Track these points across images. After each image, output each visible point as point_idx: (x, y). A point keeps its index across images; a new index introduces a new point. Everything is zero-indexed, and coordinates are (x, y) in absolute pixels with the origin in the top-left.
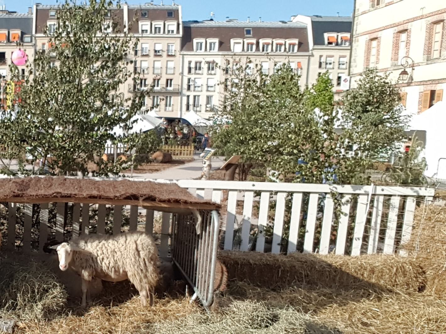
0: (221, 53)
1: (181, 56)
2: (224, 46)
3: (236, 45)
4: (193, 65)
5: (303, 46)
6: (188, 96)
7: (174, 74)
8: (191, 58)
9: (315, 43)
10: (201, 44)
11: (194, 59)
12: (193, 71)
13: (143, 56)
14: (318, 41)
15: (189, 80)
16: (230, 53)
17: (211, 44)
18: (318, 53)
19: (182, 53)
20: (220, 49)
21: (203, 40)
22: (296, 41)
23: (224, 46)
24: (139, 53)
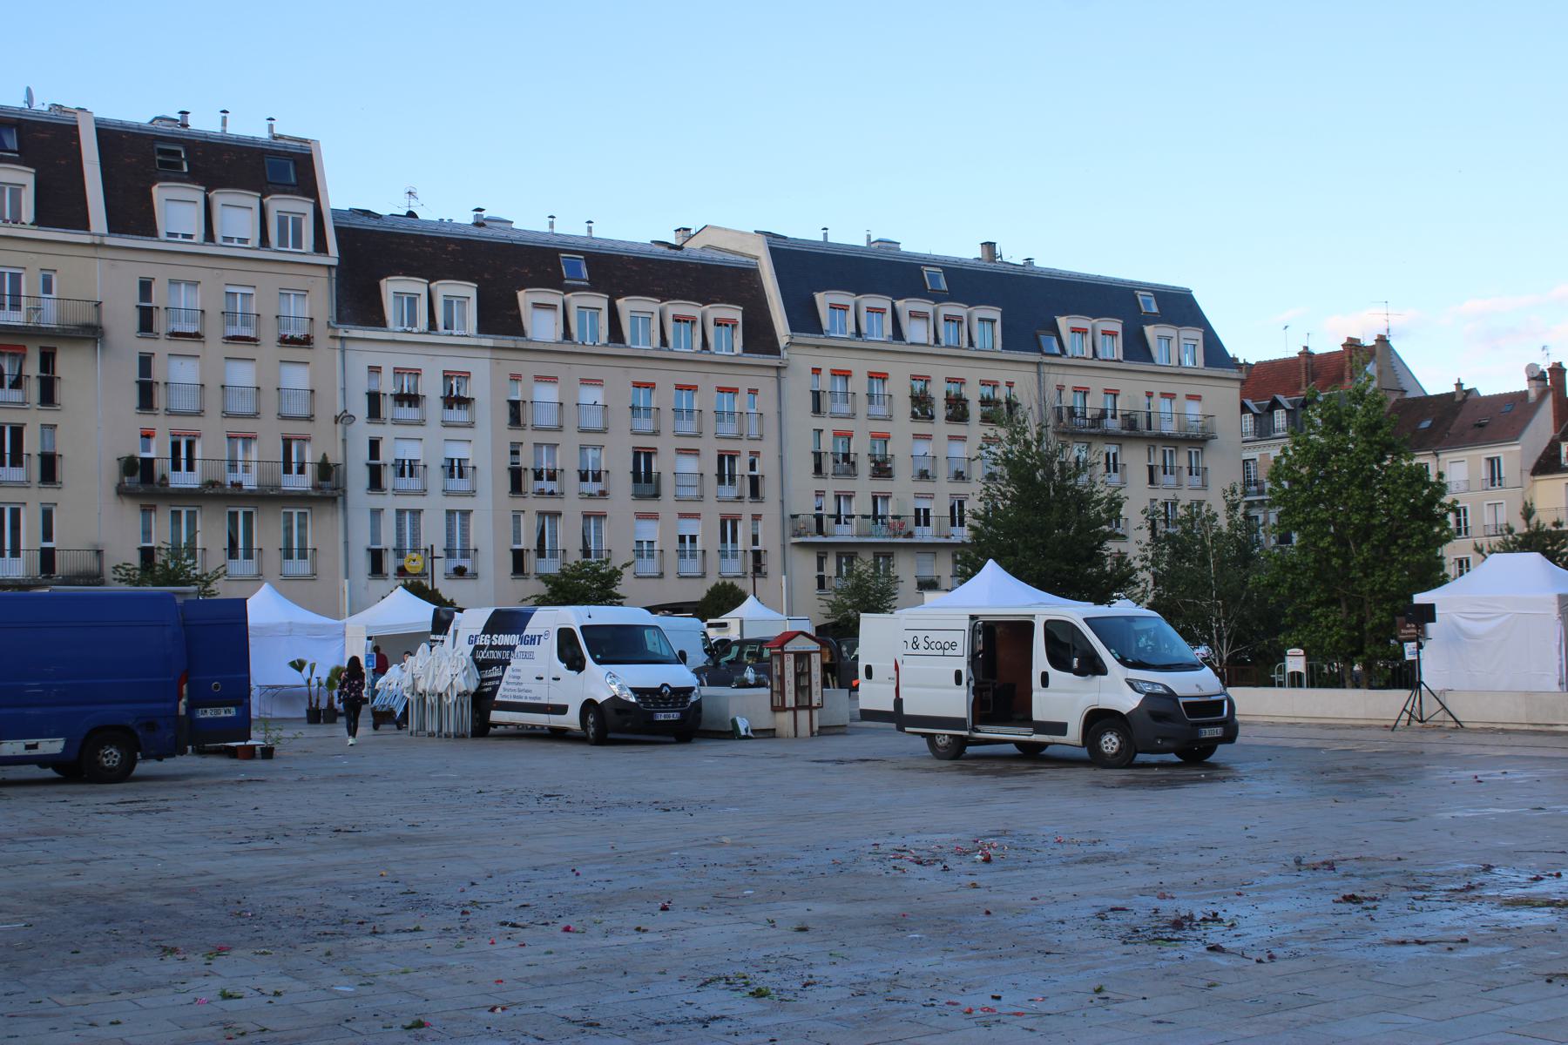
0: (488, 341)
1: (338, 344)
2: (499, 318)
3: (541, 318)
4: (387, 386)
5: (758, 337)
6: (376, 513)
7: (310, 418)
8: (369, 359)
9: (795, 326)
10: (412, 301)
11: (389, 360)
12: (387, 407)
13: (175, 335)
14: (805, 319)
15: (374, 445)
16: (521, 344)
17: (448, 303)
18: (803, 361)
19: (341, 333)
20: (484, 327)
21: (417, 286)
22: (735, 313)
23: (499, 318)
24: (161, 323)
